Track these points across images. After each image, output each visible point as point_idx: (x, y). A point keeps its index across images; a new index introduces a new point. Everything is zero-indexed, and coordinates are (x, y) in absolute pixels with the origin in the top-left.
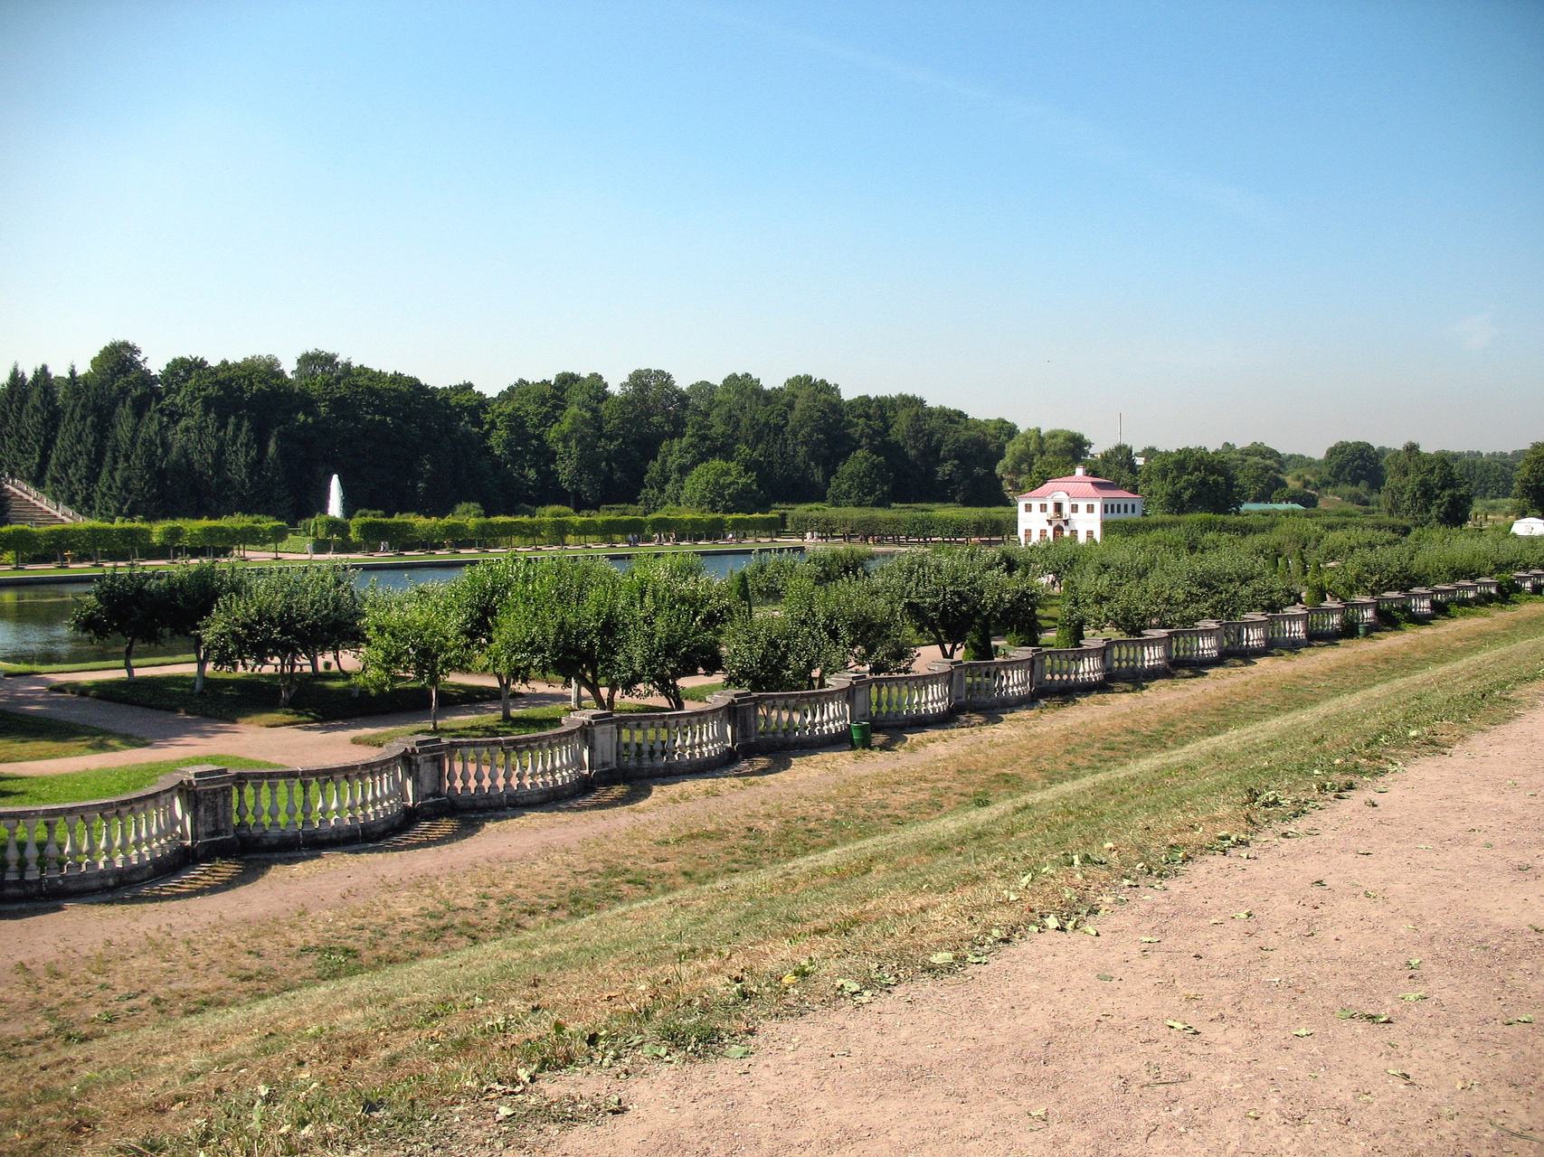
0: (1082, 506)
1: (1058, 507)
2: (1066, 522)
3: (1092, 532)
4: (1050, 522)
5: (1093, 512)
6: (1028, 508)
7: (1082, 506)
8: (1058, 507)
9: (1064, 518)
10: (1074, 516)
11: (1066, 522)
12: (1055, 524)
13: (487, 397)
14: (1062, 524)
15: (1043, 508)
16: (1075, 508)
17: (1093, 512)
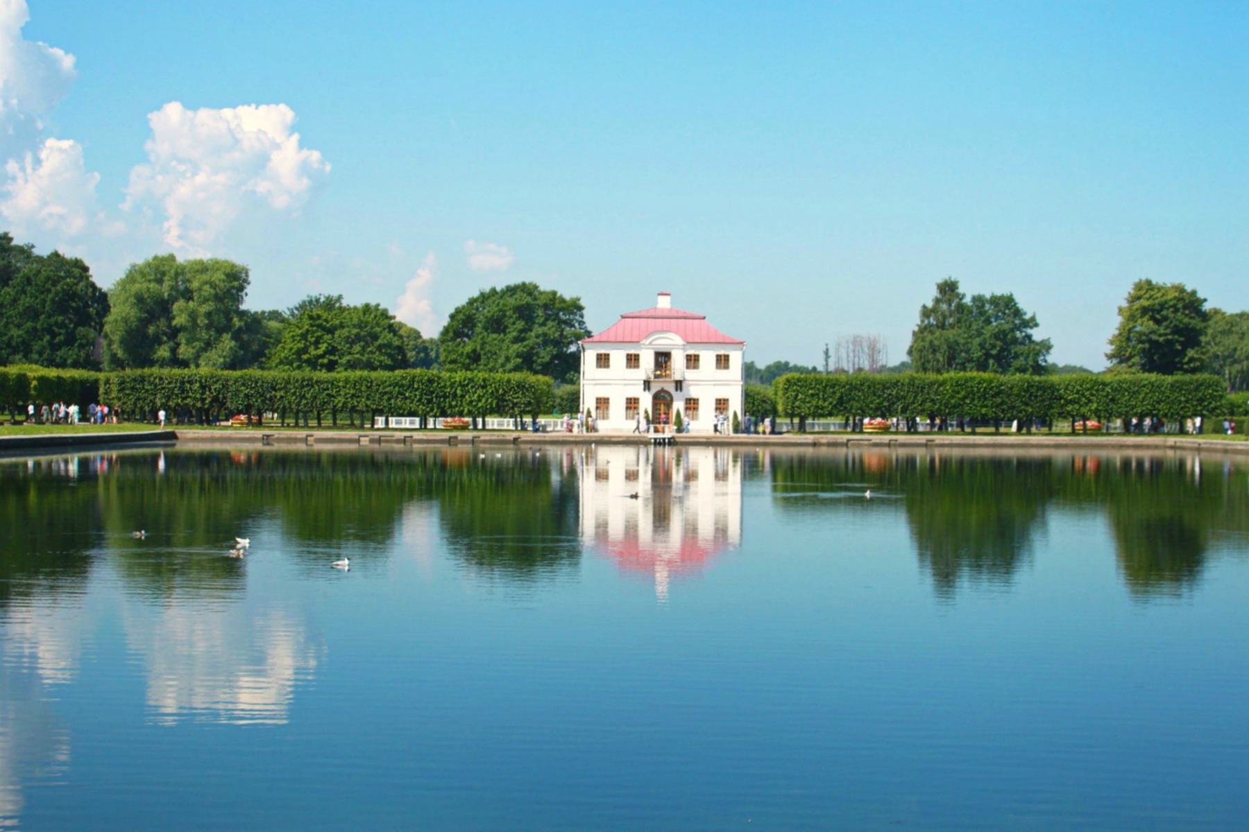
0: (708, 357)
1: (662, 359)
2: (679, 385)
3: (726, 401)
4: (647, 385)
5: (726, 367)
6: (603, 360)
7: (708, 357)
8: (662, 359)
9: (672, 379)
10: (690, 375)
11: (679, 385)
12: (655, 388)
13: (14, 243)
14: (671, 388)
15: (633, 360)
16: (692, 361)
17: (726, 367)
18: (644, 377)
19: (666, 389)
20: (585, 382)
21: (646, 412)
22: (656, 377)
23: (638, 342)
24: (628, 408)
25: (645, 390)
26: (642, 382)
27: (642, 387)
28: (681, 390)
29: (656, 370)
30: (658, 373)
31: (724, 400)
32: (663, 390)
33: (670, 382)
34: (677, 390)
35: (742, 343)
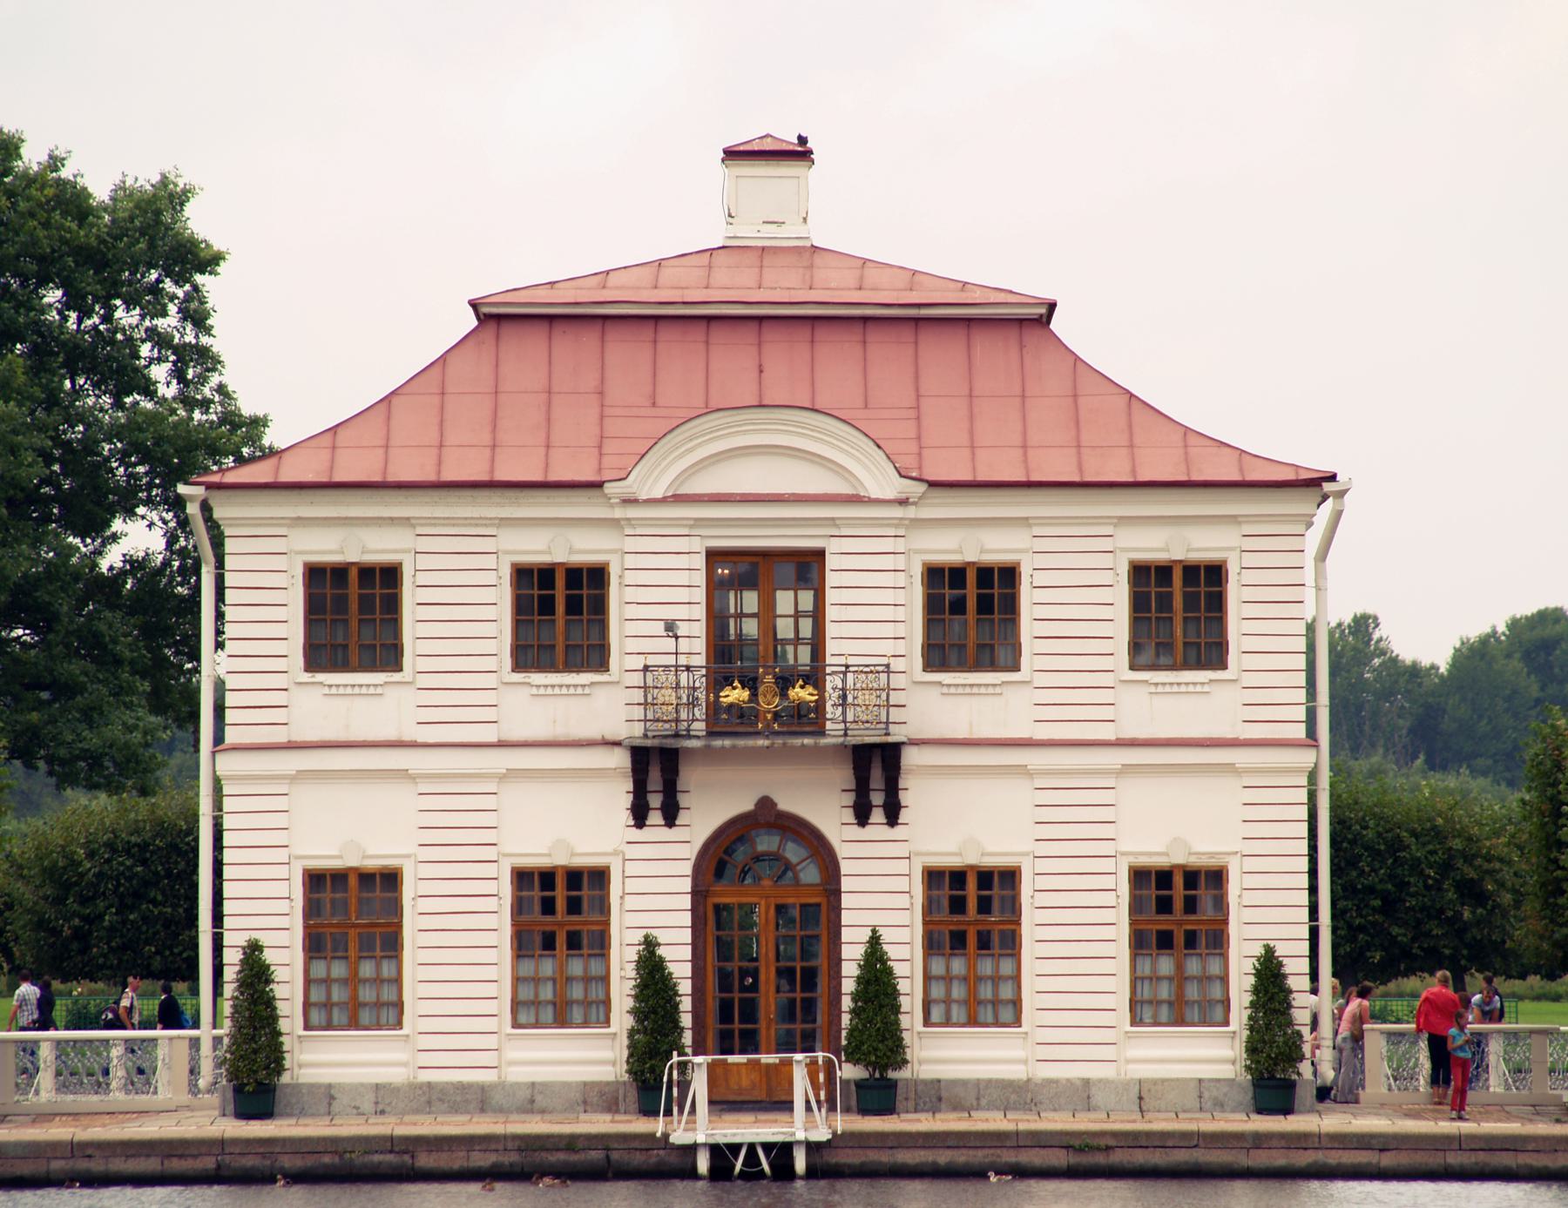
18: (638, 729)
19: (785, 804)
20: (228, 764)
21: (651, 967)
22: (725, 722)
23: (598, 485)
24: (524, 943)
25: (639, 815)
26: (620, 760)
27: (621, 795)
28: (892, 818)
29: (719, 679)
30: (735, 695)
31: (1192, 876)
32: (767, 817)
33: (818, 754)
34: (862, 817)
35: (1316, 484)
